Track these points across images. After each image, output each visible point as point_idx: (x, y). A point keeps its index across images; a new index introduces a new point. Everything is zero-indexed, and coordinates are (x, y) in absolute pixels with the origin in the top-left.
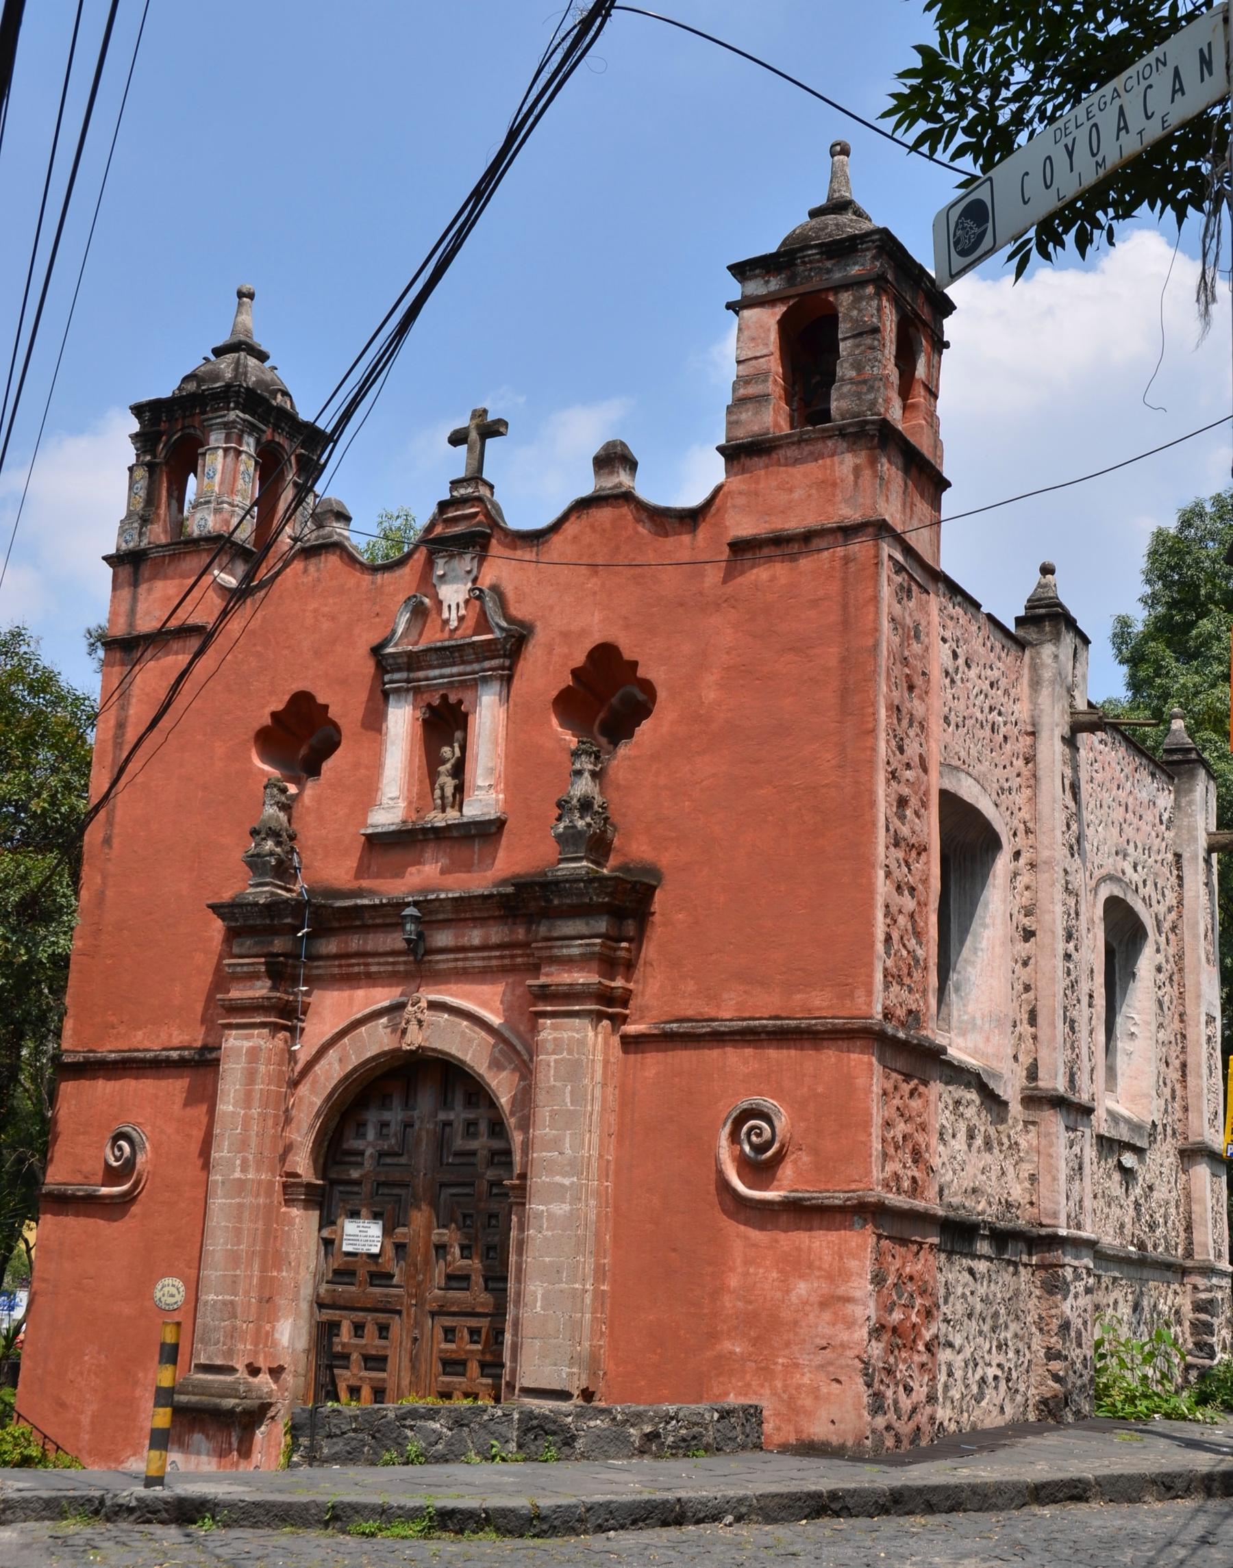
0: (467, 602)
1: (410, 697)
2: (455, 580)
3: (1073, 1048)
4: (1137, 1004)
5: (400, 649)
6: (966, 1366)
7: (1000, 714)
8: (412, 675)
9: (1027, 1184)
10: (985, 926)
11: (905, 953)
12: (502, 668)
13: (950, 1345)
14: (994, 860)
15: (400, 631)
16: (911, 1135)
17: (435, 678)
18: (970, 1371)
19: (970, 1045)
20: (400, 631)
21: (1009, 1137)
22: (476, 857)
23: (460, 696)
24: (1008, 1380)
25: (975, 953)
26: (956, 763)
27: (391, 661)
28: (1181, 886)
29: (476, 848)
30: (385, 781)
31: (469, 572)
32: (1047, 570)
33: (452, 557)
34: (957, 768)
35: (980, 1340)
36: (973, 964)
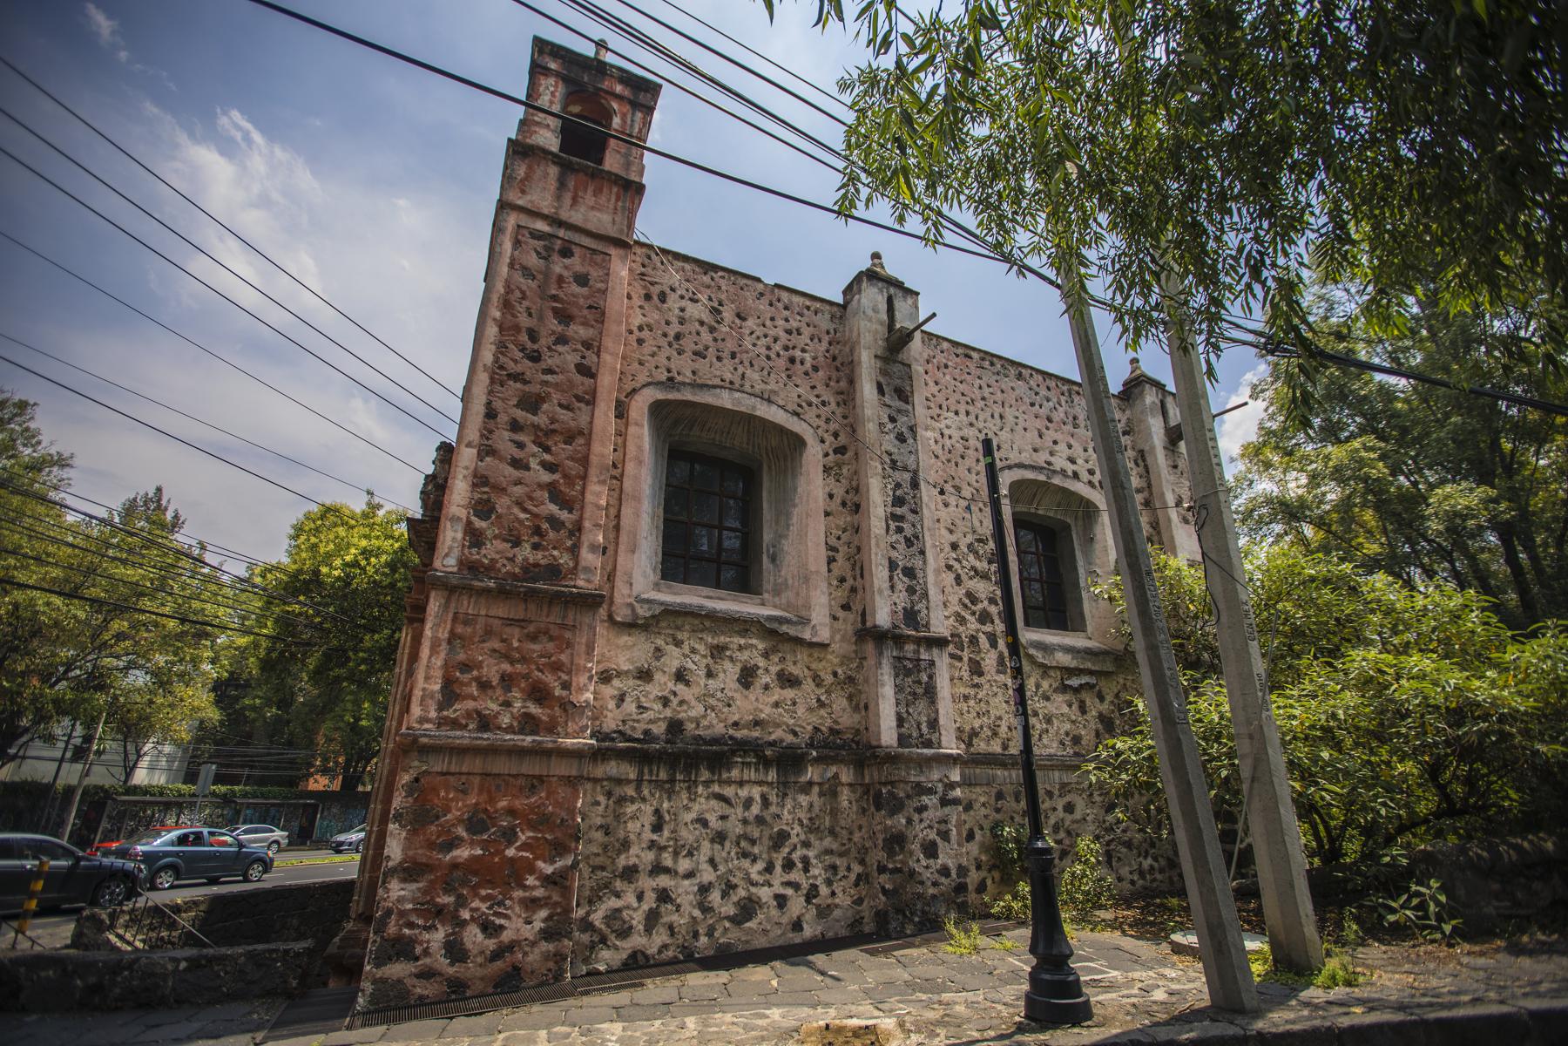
3: (911, 590)
4: (1097, 561)
6: (704, 889)
7: (803, 351)
9: (863, 713)
10: (795, 506)
11: (523, 516)
13: (667, 871)
14: (801, 455)
16: (526, 677)
18: (715, 897)
19: (784, 601)
21: (835, 674)
24: (809, 898)
25: (788, 529)
26: (717, 381)
28: (1148, 472)
32: (876, 256)
34: (715, 387)
35: (746, 863)
36: (786, 537)
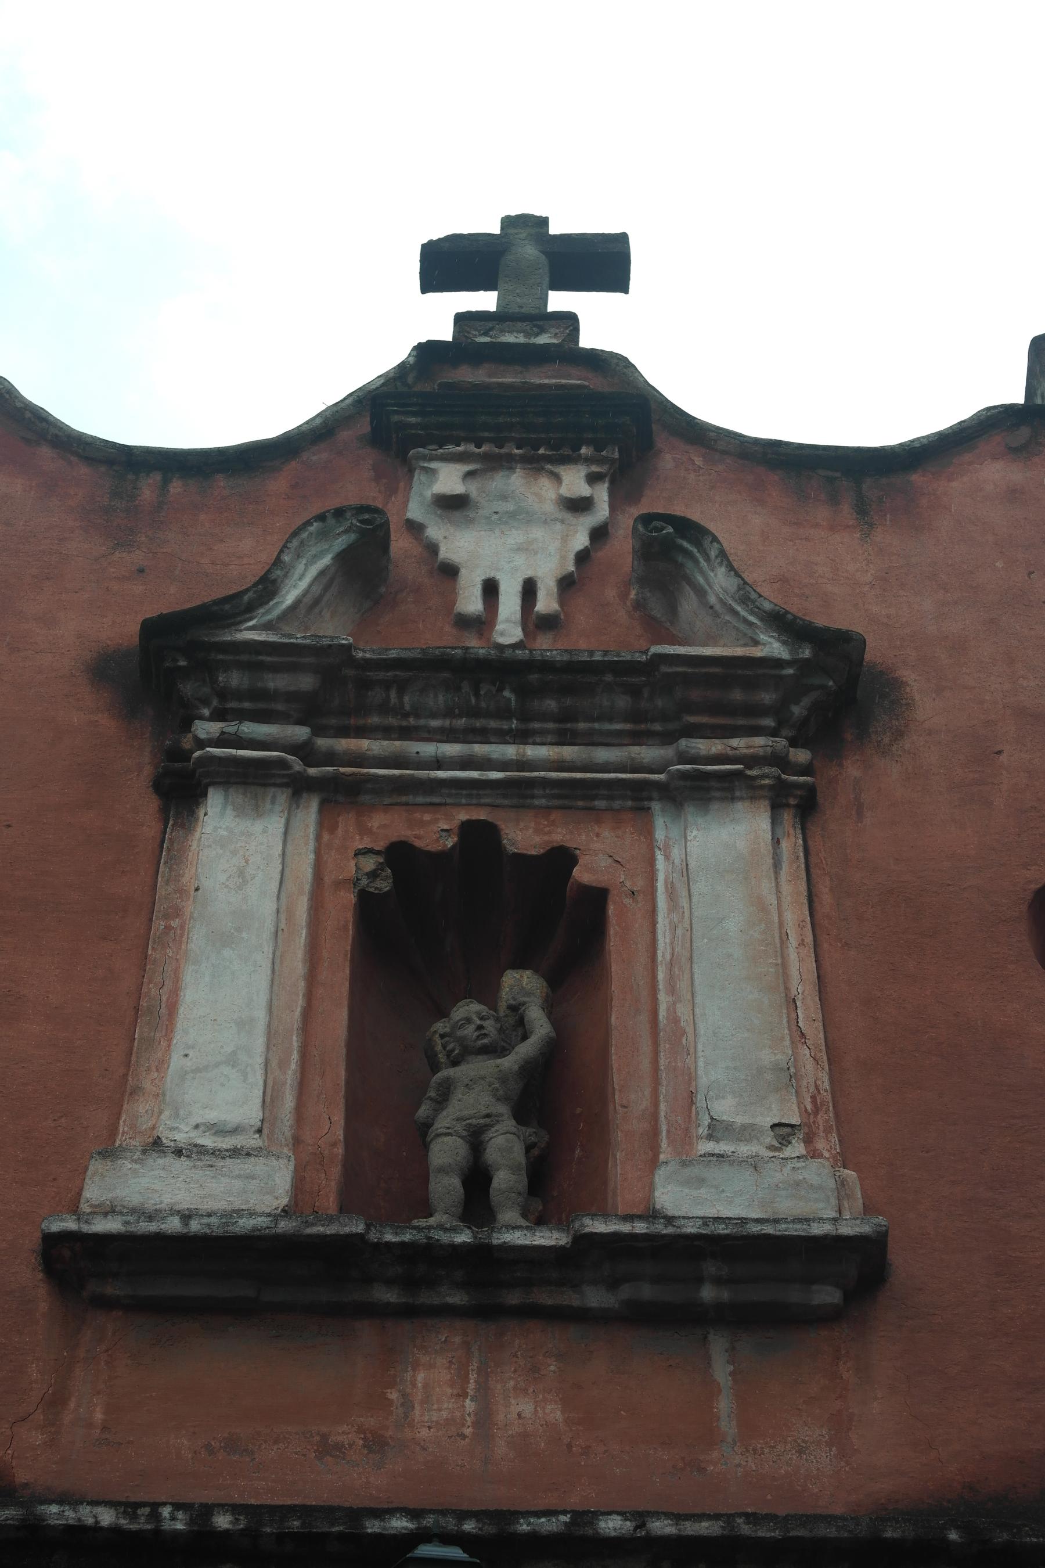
0: (566, 584)
1: (309, 814)
2: (520, 517)
5: (299, 637)
8: (323, 743)
12: (779, 760)
15: (289, 596)
17: (439, 764)
20: (289, 596)
22: (724, 1405)
23: (560, 836)
27: (235, 679)
29: (721, 1372)
30: (176, 1061)
31: (579, 506)
33: (495, 463)
